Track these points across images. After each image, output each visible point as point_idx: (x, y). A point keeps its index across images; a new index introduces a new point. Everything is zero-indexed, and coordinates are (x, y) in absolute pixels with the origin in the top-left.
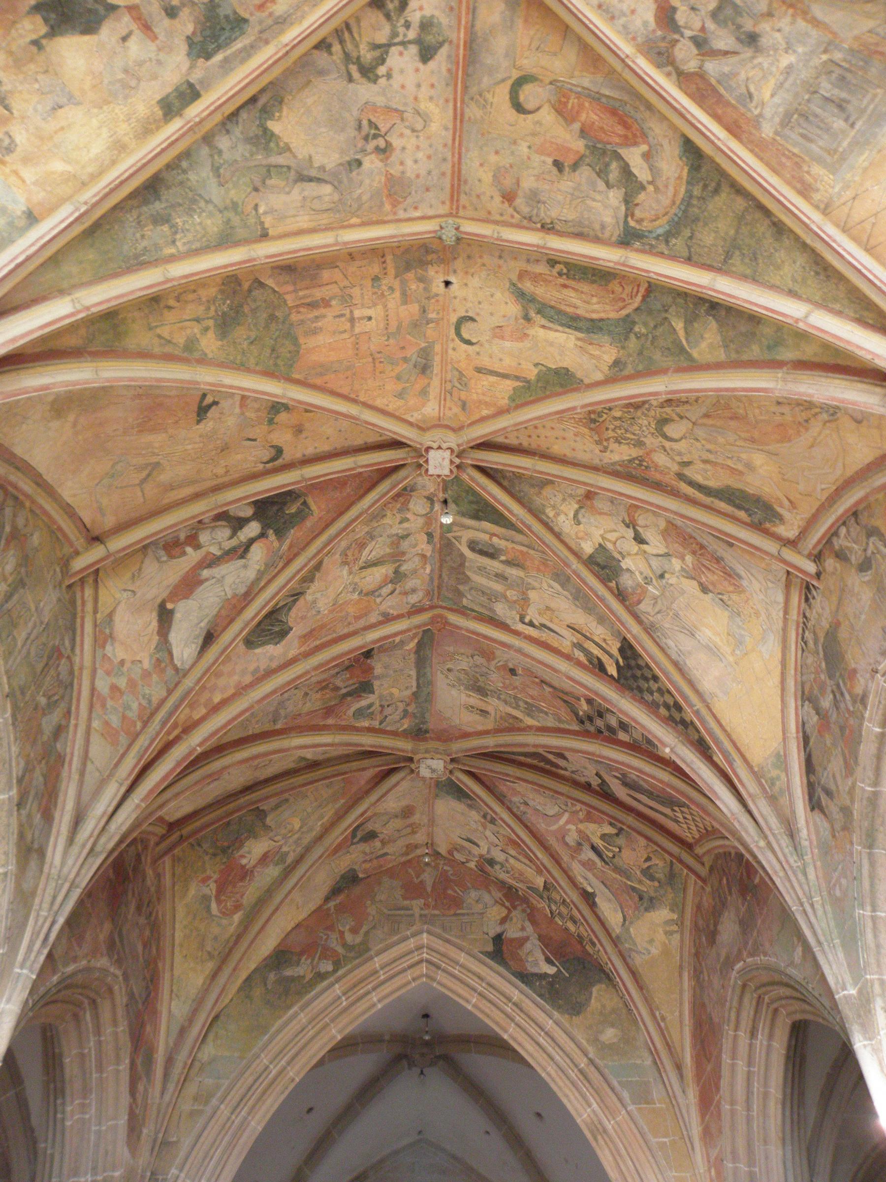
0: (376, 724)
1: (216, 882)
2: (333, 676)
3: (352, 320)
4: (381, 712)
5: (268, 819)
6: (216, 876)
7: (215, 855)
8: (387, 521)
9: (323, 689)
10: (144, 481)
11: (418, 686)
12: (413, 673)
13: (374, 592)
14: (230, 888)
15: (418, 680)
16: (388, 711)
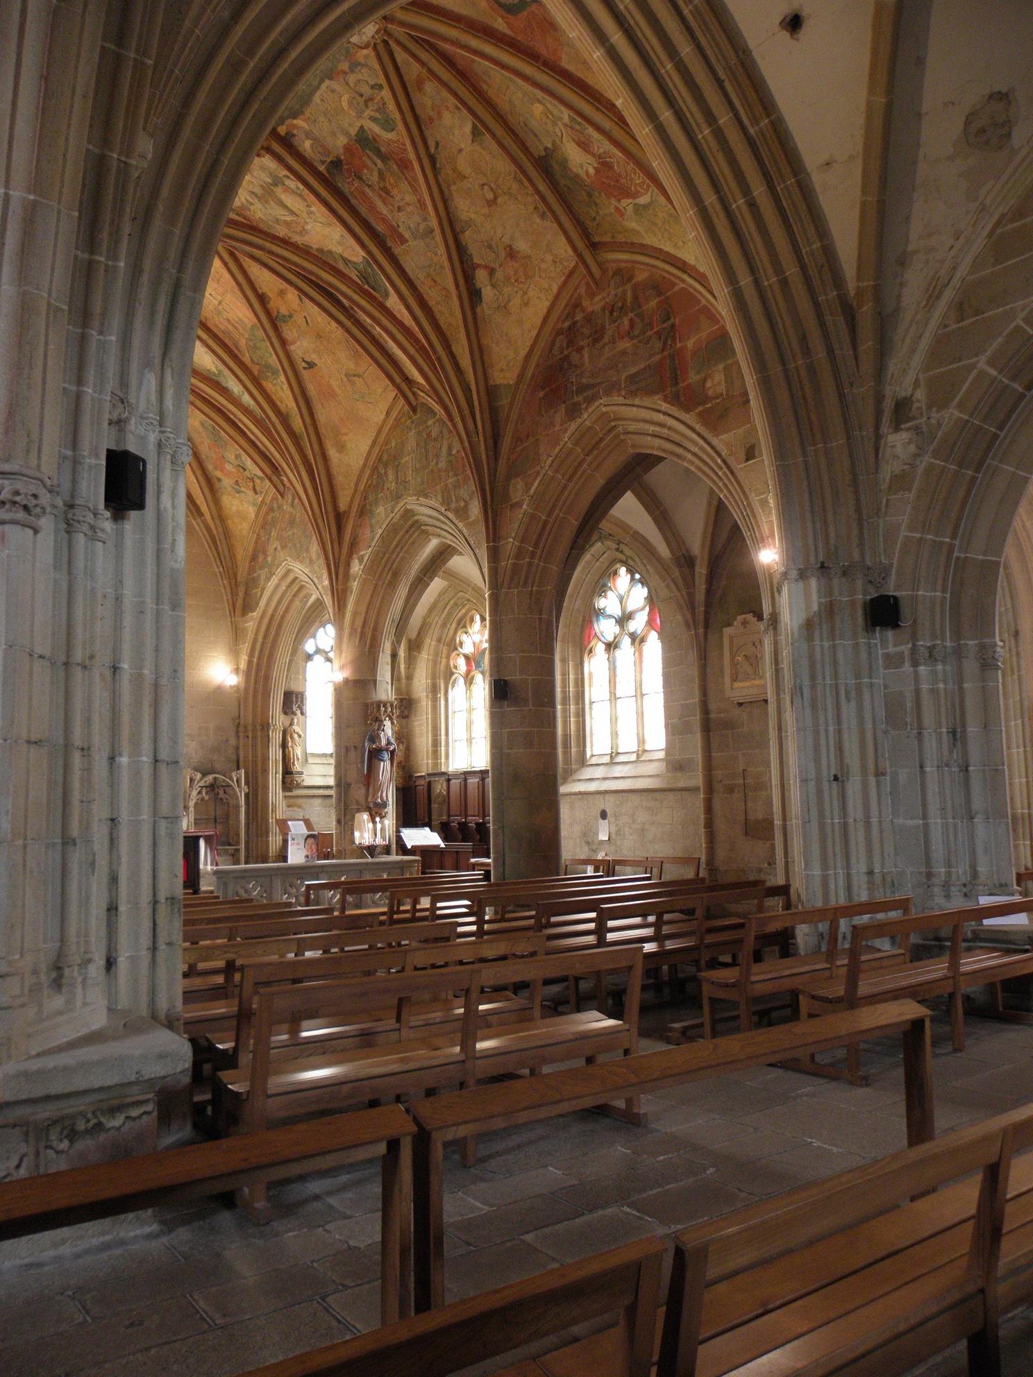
0: (386, 93)
1: (619, 201)
2: (373, 190)
3: (220, 303)
4: (371, 99)
5: (549, 145)
6: (614, 202)
7: (596, 204)
8: (259, 215)
9: (388, 192)
10: (358, 376)
11: (321, 82)
12: (316, 98)
13: (300, 195)
14: (623, 181)
15: (318, 87)
16: (366, 90)
